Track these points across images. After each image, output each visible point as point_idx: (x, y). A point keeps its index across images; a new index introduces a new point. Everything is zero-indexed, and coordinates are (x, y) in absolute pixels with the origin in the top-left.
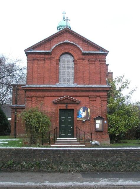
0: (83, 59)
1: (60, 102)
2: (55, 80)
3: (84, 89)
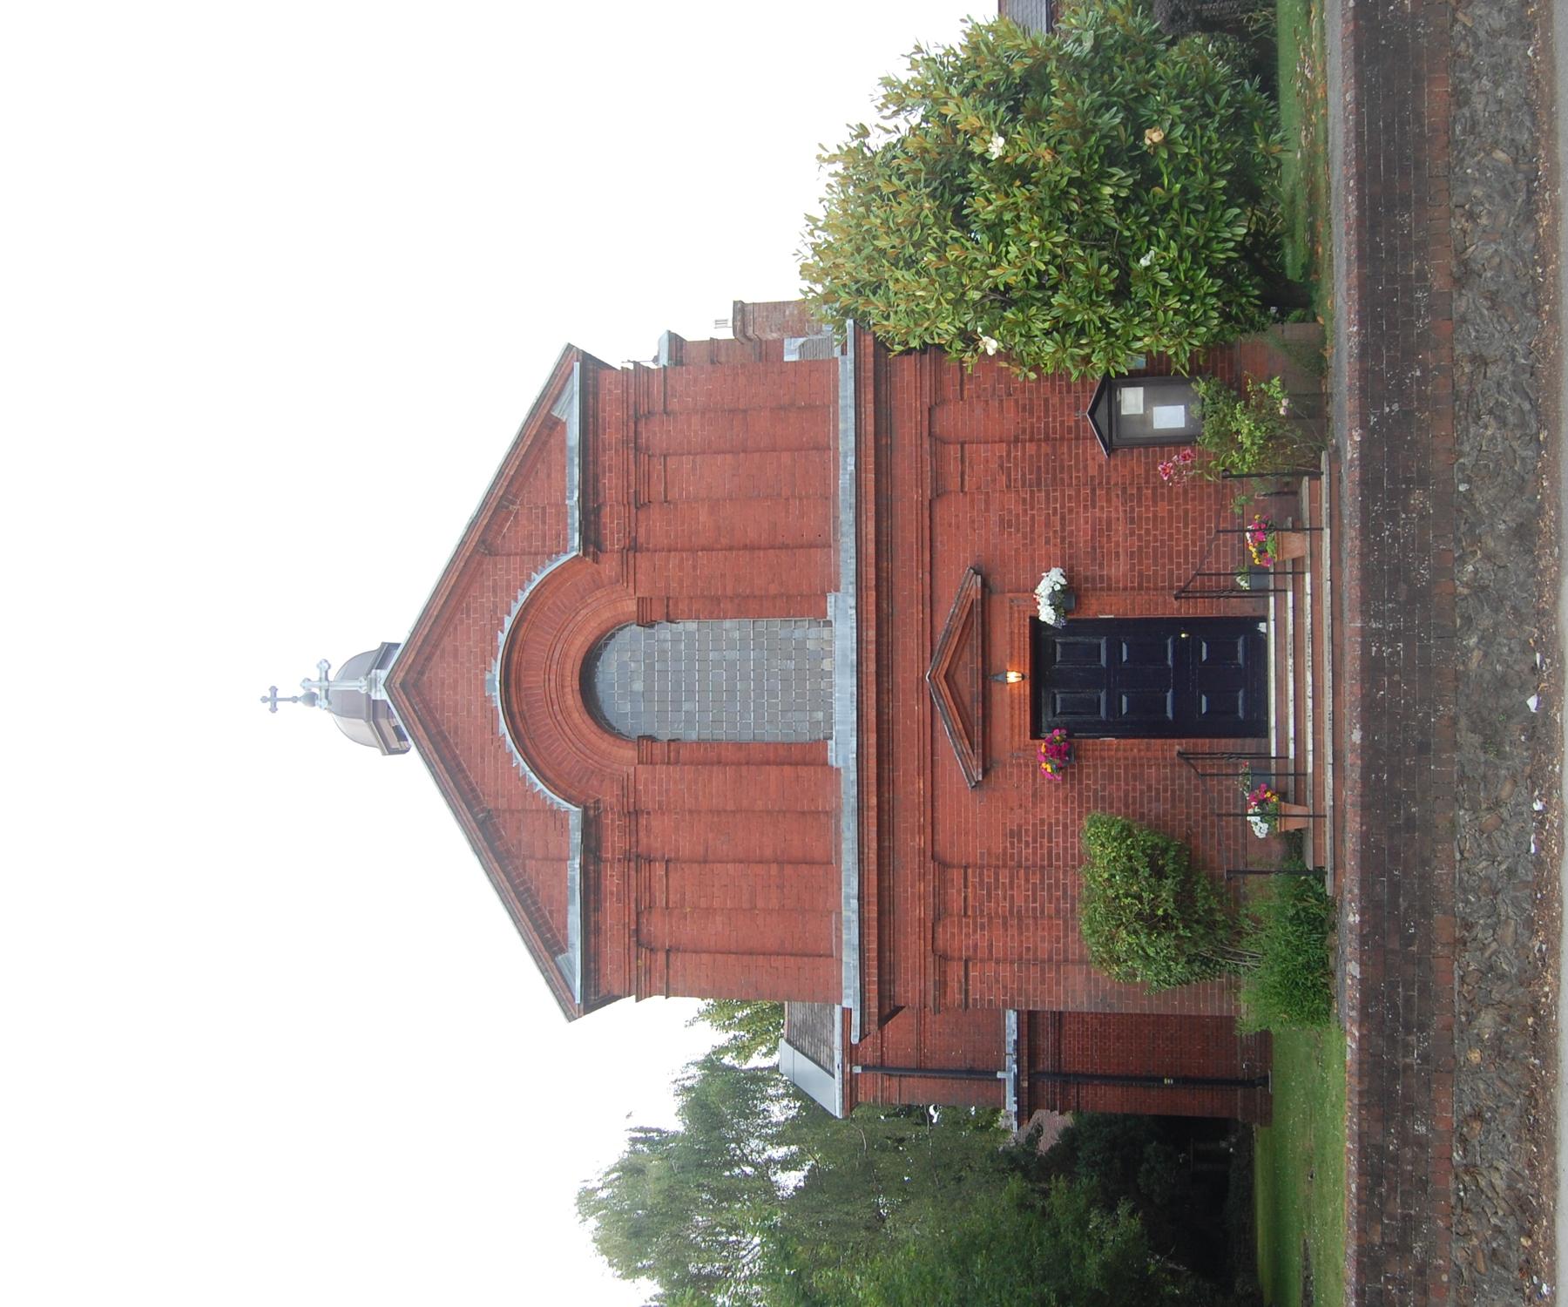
0: (633, 547)
1: (978, 729)
2: (803, 771)
3: (872, 536)
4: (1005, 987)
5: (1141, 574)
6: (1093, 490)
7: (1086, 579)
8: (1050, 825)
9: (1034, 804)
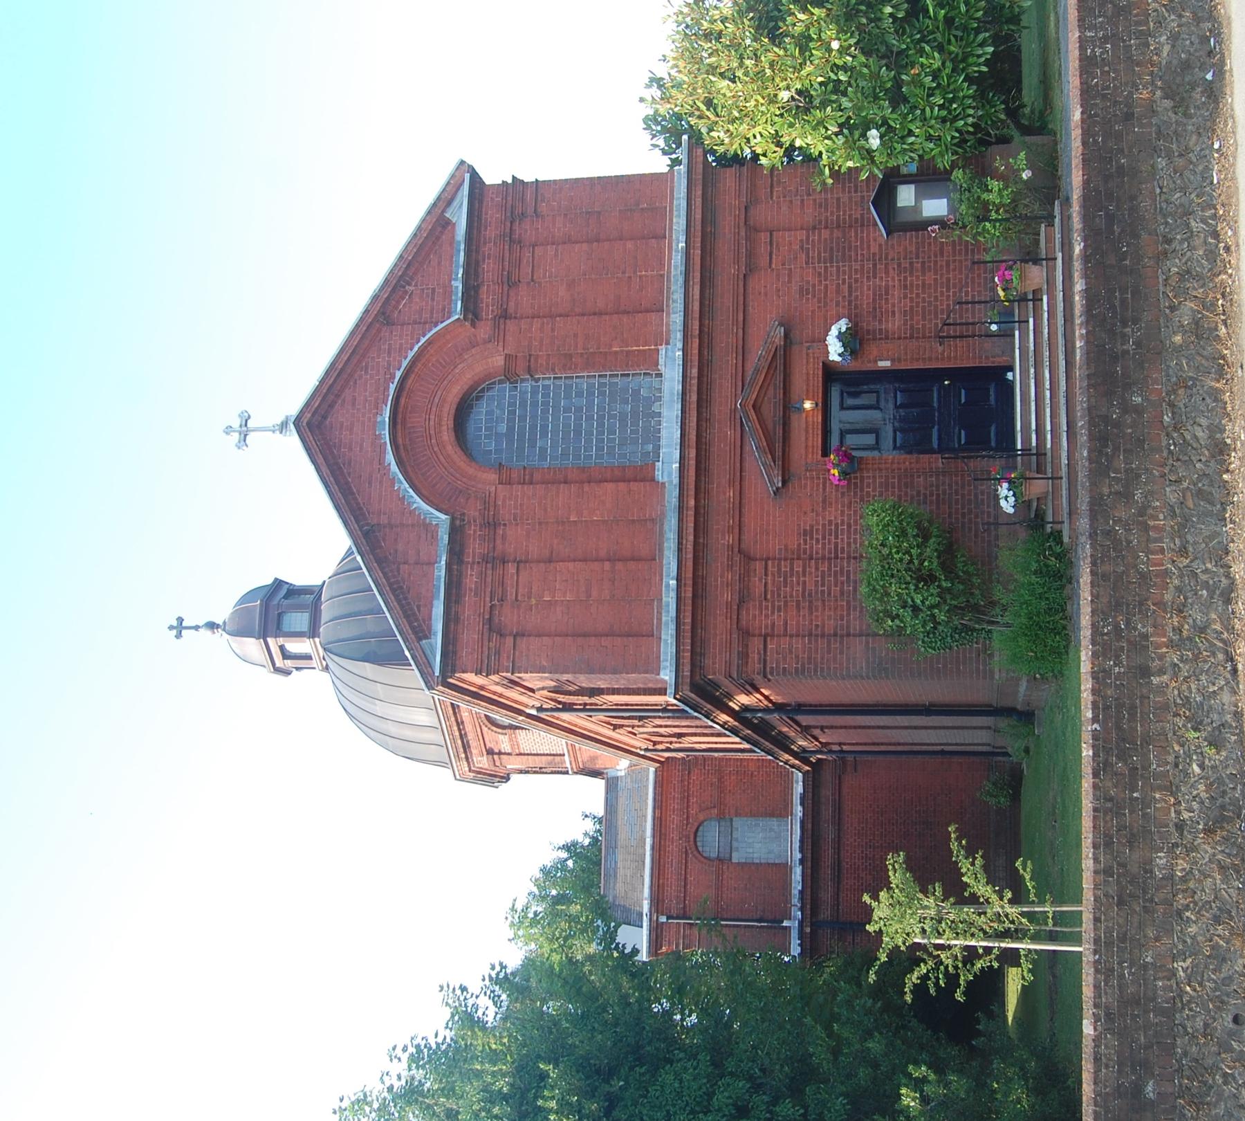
0: (505, 315)
1: (778, 447)
2: (634, 486)
3: (697, 296)
4: (797, 657)
5: (912, 327)
6: (875, 265)
7: (868, 331)
8: (837, 525)
9: (824, 509)
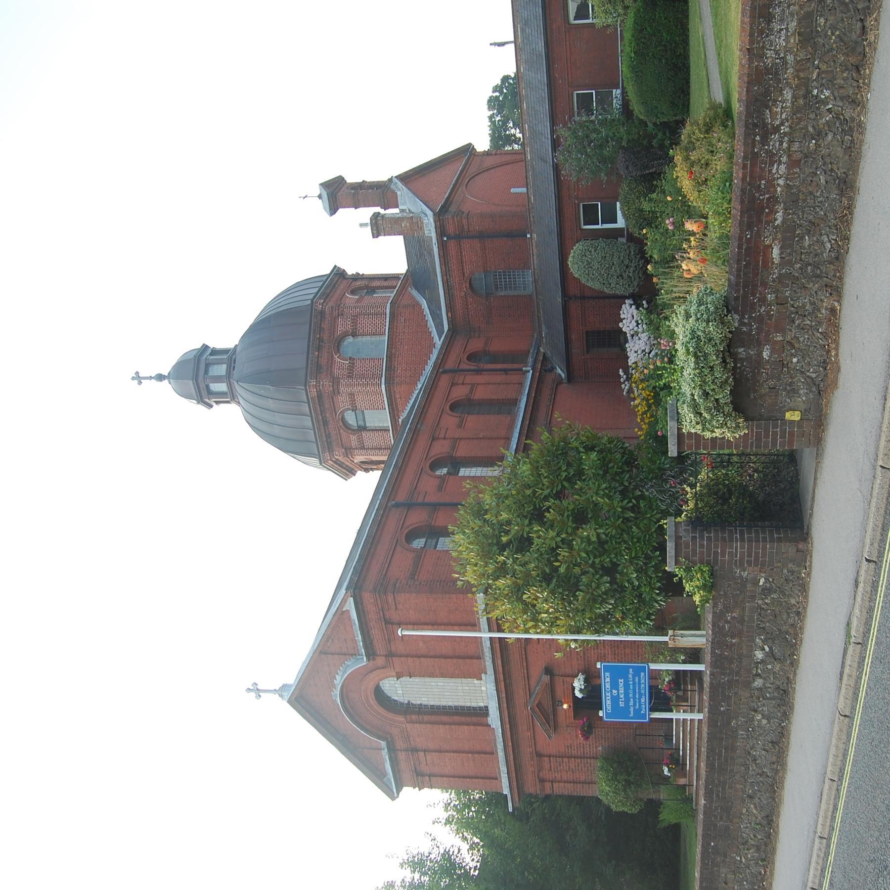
0: (390, 655)
2: (478, 728)
